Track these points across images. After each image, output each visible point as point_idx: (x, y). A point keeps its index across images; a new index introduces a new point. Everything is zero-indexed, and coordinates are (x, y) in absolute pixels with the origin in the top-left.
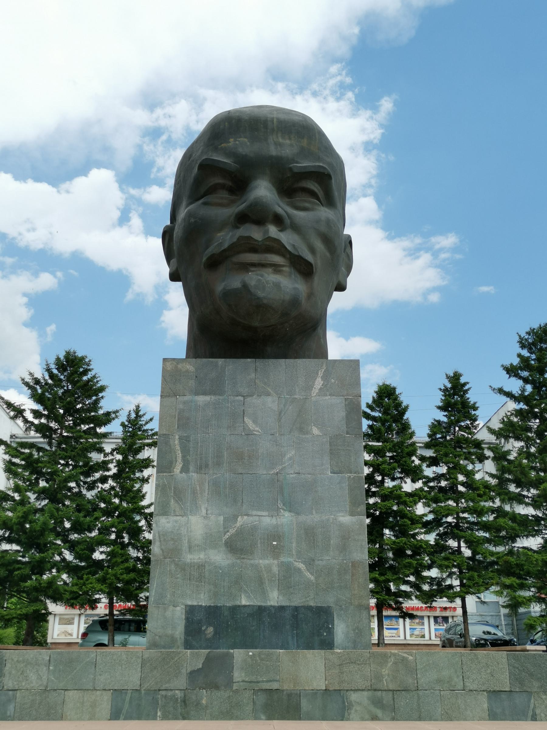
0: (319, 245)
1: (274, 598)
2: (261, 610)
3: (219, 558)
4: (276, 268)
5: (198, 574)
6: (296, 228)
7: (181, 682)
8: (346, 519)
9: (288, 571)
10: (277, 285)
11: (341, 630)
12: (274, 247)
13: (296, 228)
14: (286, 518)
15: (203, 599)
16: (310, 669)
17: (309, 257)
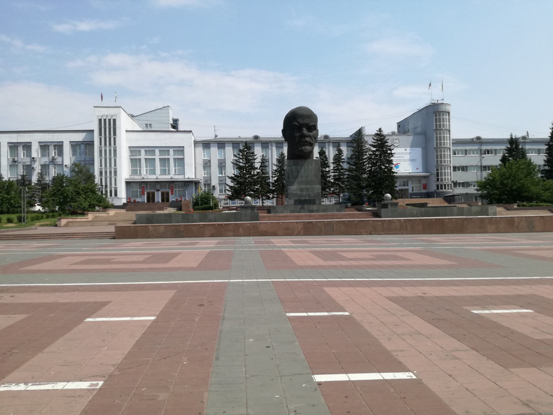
0: (314, 139)
1: (307, 198)
2: (305, 200)
3: (299, 192)
4: (307, 146)
5: (296, 195)
6: (310, 137)
7: (299, 209)
8: (318, 186)
9: (309, 194)
10: (307, 149)
11: (317, 202)
12: (307, 142)
13: (310, 137)
14: (308, 186)
15: (296, 198)
16: (315, 207)
17: (312, 142)
